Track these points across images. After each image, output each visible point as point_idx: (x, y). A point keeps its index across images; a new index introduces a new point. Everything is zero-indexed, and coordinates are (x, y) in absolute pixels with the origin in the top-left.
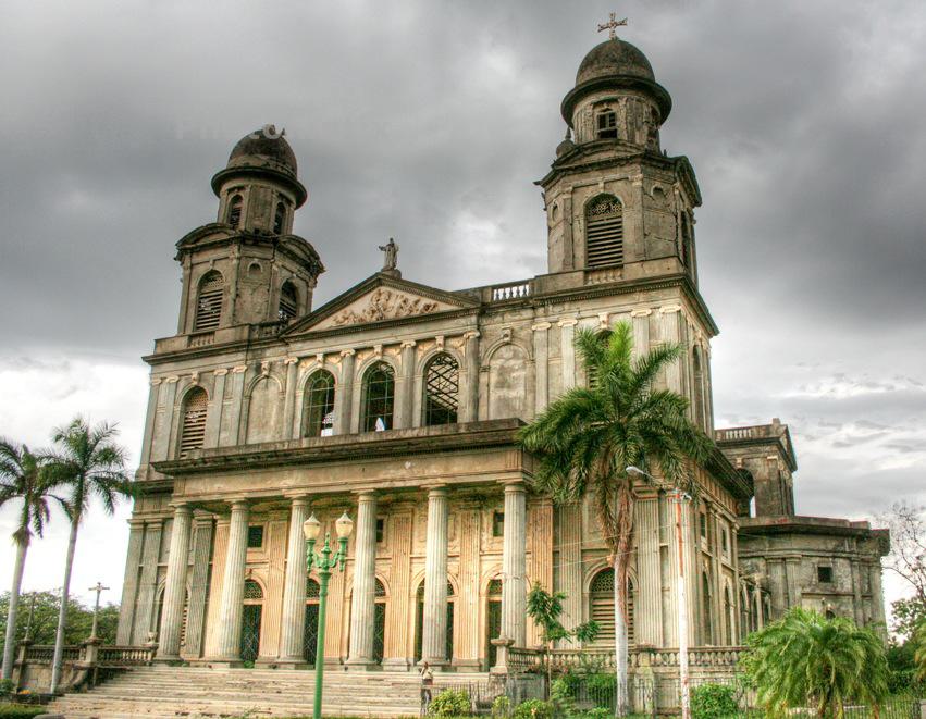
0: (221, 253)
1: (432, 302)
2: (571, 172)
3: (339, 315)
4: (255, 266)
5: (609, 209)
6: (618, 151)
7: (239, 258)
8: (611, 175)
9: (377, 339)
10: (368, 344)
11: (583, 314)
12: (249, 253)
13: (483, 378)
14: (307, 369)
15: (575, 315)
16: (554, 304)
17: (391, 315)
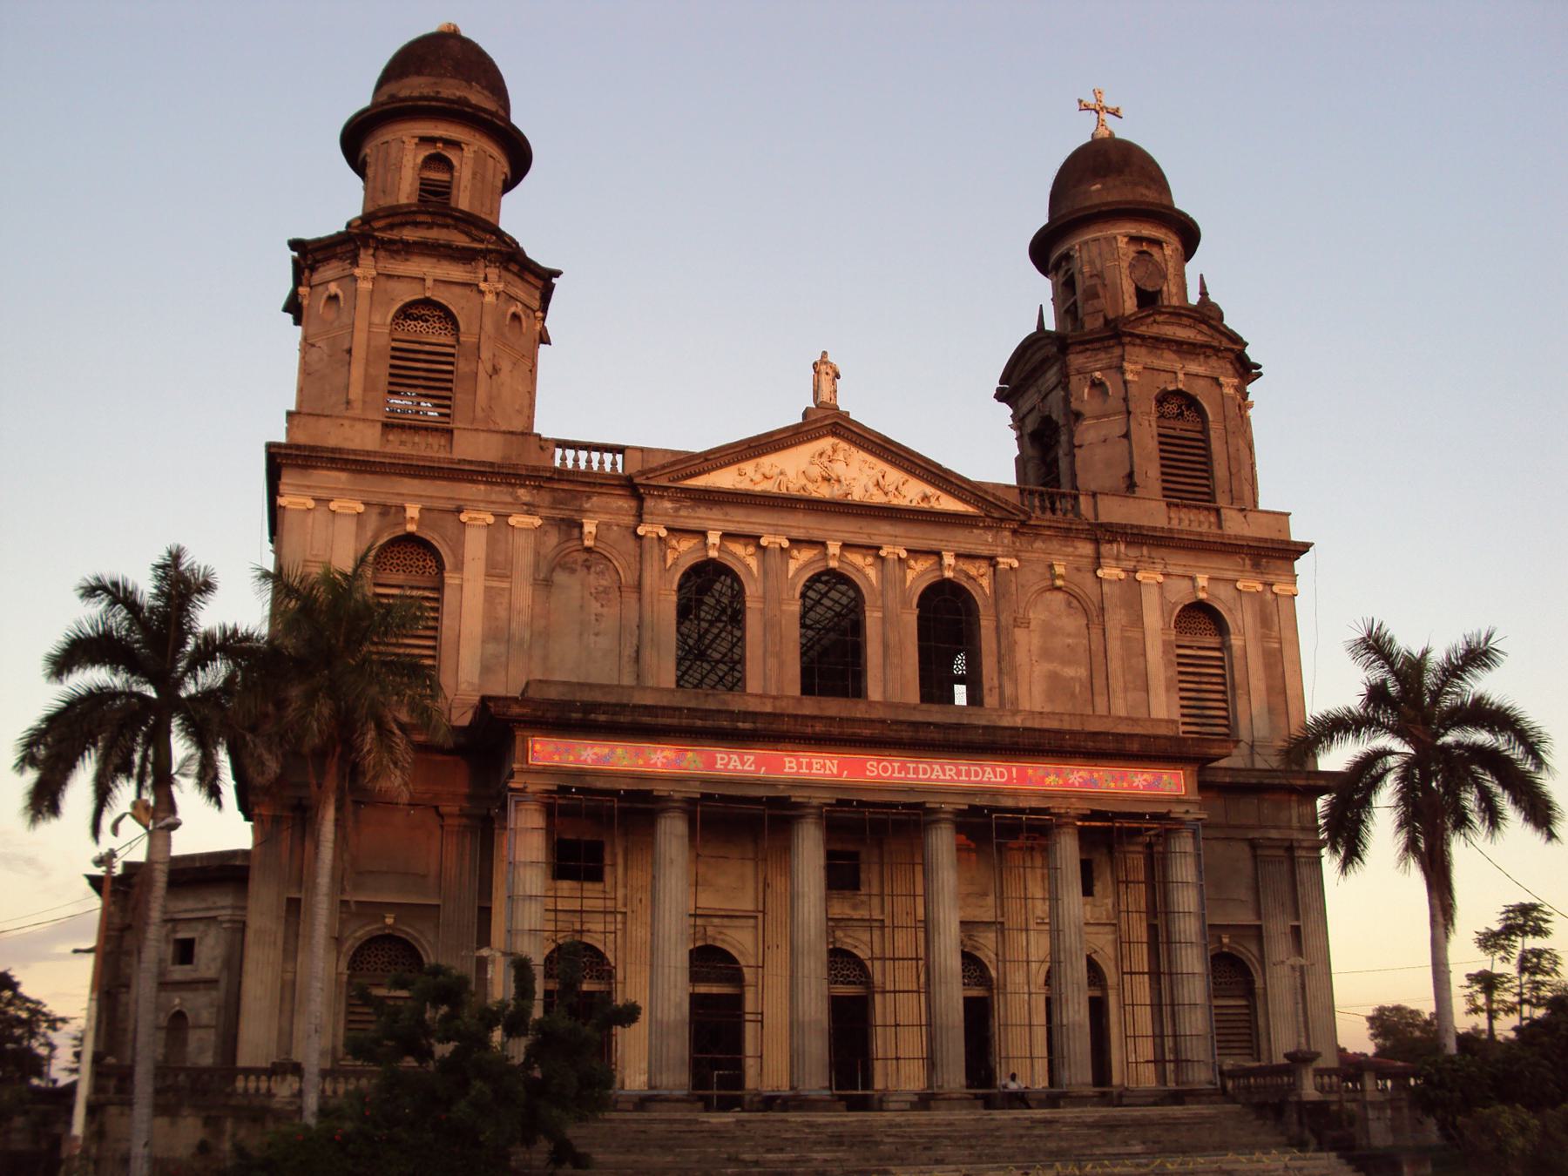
0: (456, 272)
1: (930, 490)
2: (1138, 341)
3: (748, 467)
4: (515, 317)
5: (1181, 414)
6: (1200, 332)
7: (498, 294)
8: (1193, 368)
9: (835, 534)
10: (817, 535)
11: (1170, 569)
12: (513, 291)
13: (1020, 635)
14: (685, 552)
15: (1160, 567)
16: (1128, 544)
17: (857, 495)
